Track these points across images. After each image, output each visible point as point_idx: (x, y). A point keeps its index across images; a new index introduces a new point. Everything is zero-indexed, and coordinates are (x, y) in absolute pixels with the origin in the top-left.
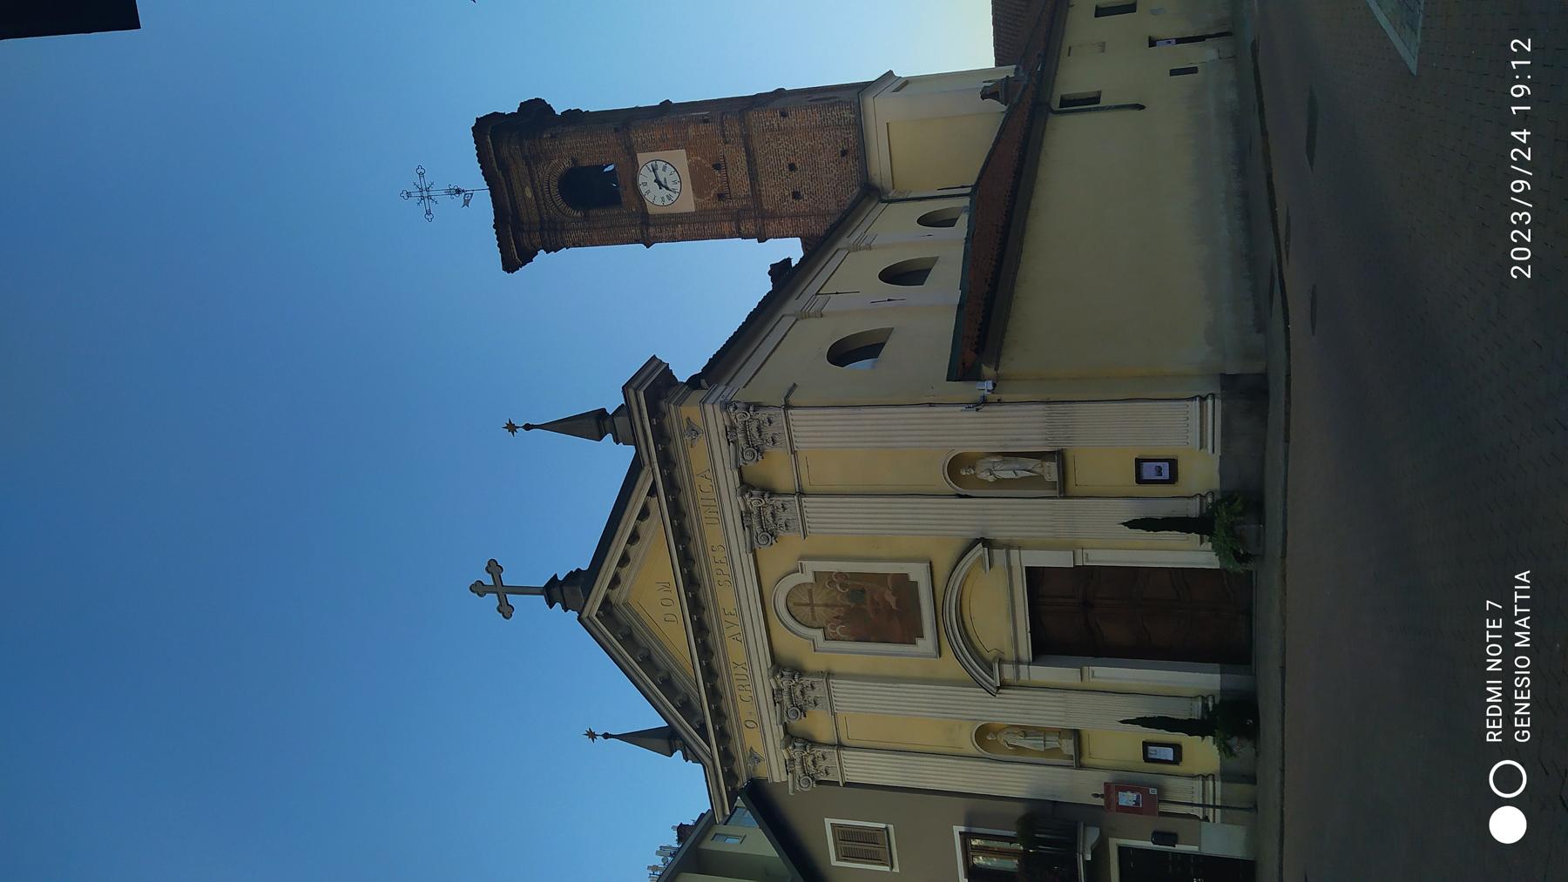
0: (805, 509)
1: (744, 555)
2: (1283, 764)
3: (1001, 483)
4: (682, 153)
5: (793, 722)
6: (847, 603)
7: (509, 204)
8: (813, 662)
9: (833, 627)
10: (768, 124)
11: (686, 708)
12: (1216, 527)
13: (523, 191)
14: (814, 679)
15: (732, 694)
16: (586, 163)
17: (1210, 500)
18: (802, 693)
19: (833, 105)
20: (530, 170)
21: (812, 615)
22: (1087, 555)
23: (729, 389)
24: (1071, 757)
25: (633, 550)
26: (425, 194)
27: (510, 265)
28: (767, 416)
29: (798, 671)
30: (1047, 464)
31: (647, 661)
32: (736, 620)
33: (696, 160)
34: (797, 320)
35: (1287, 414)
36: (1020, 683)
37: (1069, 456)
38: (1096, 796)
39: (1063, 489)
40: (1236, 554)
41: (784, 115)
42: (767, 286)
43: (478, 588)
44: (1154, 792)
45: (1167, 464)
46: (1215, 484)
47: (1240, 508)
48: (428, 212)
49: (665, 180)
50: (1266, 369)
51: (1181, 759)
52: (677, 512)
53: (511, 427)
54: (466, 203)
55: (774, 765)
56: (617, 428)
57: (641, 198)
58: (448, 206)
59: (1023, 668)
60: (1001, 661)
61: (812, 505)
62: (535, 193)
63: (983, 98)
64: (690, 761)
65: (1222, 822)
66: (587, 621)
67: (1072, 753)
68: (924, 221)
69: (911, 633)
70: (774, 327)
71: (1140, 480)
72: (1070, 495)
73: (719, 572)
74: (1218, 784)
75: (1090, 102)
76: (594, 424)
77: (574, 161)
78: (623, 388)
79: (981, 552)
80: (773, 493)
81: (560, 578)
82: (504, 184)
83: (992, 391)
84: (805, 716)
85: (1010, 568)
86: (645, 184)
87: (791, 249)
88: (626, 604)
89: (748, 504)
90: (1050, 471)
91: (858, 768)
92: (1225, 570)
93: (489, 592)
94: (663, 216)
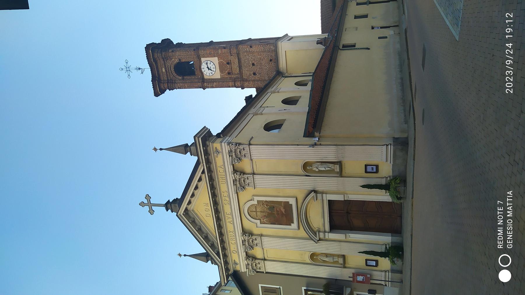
0: (255, 179)
1: (234, 195)
2: (411, 267)
3: (320, 172)
6: (268, 211)
7: (157, 75)
8: (256, 231)
10: (245, 50)
11: (213, 246)
12: (390, 188)
13: (162, 69)
14: (257, 237)
15: (228, 242)
16: (184, 61)
17: (389, 179)
18: (252, 241)
19: (267, 44)
22: (348, 196)
23: (230, 138)
24: (342, 264)
25: (196, 192)
26: (128, 69)
27: (157, 94)
29: (251, 234)
30: (336, 166)
31: (200, 230)
34: (254, 115)
35: (414, 151)
37: (343, 164)
38: (350, 277)
39: (341, 174)
40: (397, 197)
41: (251, 47)
42: (244, 104)
43: (142, 204)
44: (369, 276)
45: (375, 166)
46: (391, 174)
47: (399, 182)
48: (129, 75)
49: (210, 67)
50: (408, 136)
51: (378, 265)
52: (211, 179)
53: (155, 149)
54: (142, 73)
55: (242, 266)
56: (192, 152)
58: (136, 74)
59: (326, 234)
60: (319, 232)
62: (166, 71)
63: (317, 44)
64: (213, 264)
65: (391, 286)
66: (179, 216)
67: (342, 263)
68: (297, 84)
69: (289, 222)
70: (246, 117)
72: (343, 176)
73: (225, 200)
74: (390, 274)
75: (352, 46)
76: (184, 149)
77: (180, 60)
78: (194, 137)
79: (313, 195)
80: (244, 173)
81: (171, 201)
83: (318, 141)
84: (253, 249)
85: (323, 200)
86: (204, 68)
87: (253, 92)
88: (193, 210)
90: (337, 168)
91: (271, 267)
92: (394, 202)
94: (209, 79)
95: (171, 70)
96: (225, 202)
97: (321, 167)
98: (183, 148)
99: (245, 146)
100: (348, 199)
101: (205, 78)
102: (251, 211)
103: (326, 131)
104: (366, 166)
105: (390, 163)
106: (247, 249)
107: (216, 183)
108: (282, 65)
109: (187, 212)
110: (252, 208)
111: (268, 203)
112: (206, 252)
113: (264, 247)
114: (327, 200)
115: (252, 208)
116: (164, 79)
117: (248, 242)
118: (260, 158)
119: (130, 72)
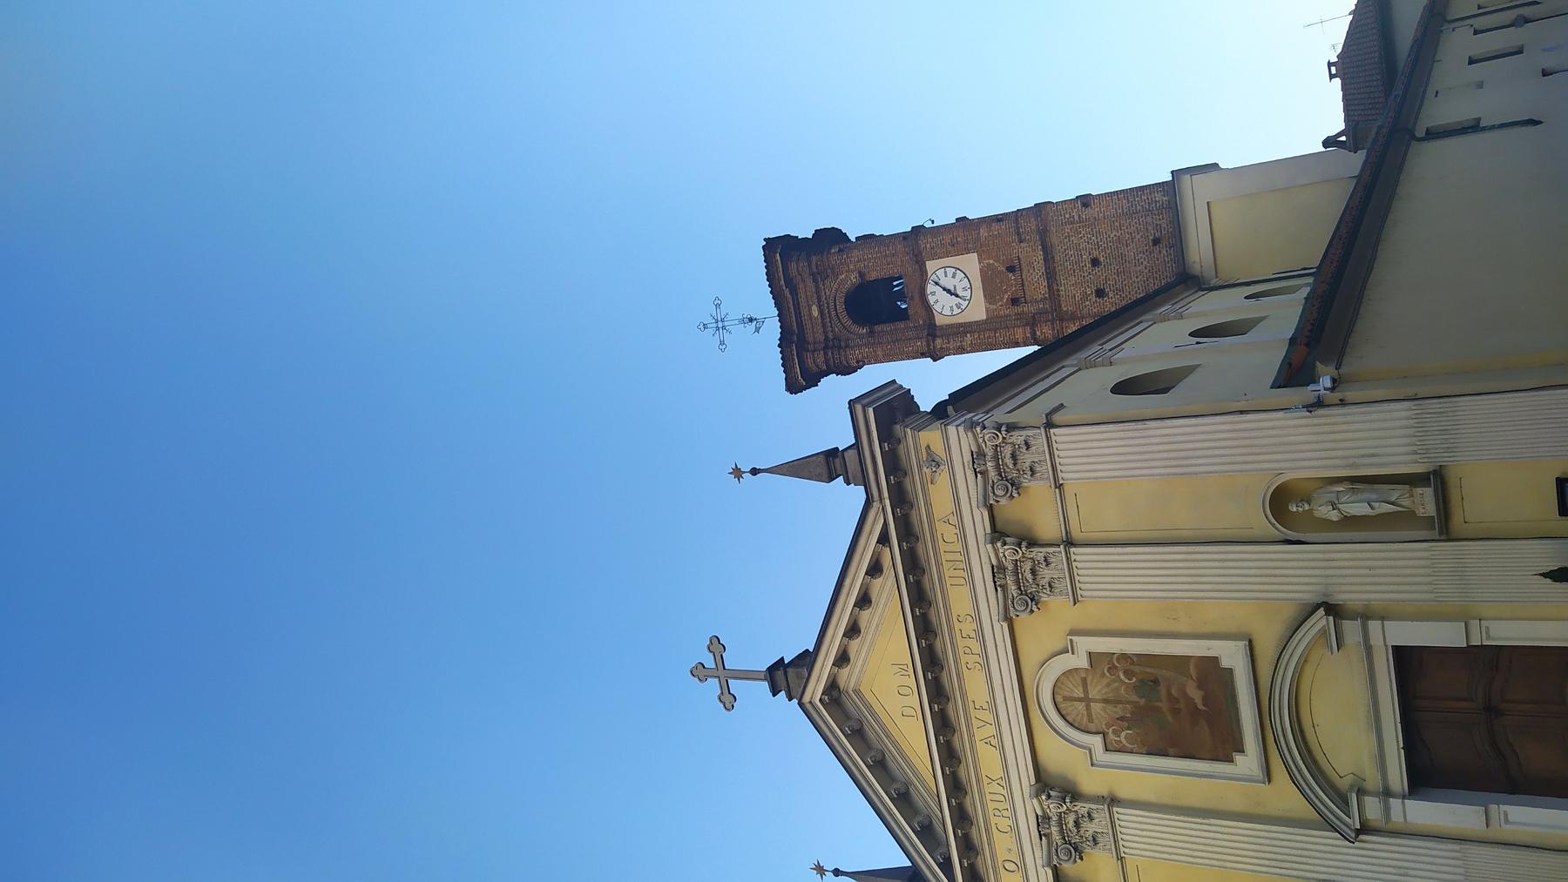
3: (1349, 522)
5: (1065, 865)
6: (1138, 700)
8: (1091, 781)
10: (1067, 216)
11: (927, 832)
13: (810, 310)
14: (1094, 806)
16: (873, 276)
18: (1077, 824)
20: (817, 287)
22: (1487, 628)
26: (720, 324)
27: (793, 387)
28: (1023, 438)
29: (1071, 793)
30: (1419, 490)
31: (880, 766)
32: (989, 718)
33: (989, 264)
36: (1390, 827)
37: (1452, 480)
39: (1443, 526)
43: (699, 672)
48: (722, 343)
49: (955, 287)
52: (914, 566)
53: (737, 473)
54: (757, 330)
57: (928, 309)
58: (740, 335)
59: (1395, 803)
60: (1361, 792)
61: (1084, 558)
62: (821, 312)
66: (809, 706)
69: (1225, 746)
73: (968, 651)
76: (828, 465)
77: (861, 275)
79: (1323, 622)
80: (1033, 543)
82: (791, 303)
83: (1333, 389)
84: (1081, 859)
85: (1368, 649)
86: (933, 293)
88: (857, 692)
89: (1001, 555)
93: (711, 677)
94: (951, 326)
95: (836, 310)
96: (971, 659)
97: (1352, 499)
98: (822, 459)
99: (1030, 432)
101: (937, 324)
102: (1066, 699)
103: (1365, 356)
106: (1057, 856)
107: (931, 582)
108: (1199, 250)
109: (835, 693)
110: (1071, 686)
111: (1133, 663)
112: (911, 865)
113: (1126, 850)
114: (1386, 646)
115: (1071, 686)
116: (815, 338)
117: (1060, 825)
118: (1088, 475)
119: (725, 331)
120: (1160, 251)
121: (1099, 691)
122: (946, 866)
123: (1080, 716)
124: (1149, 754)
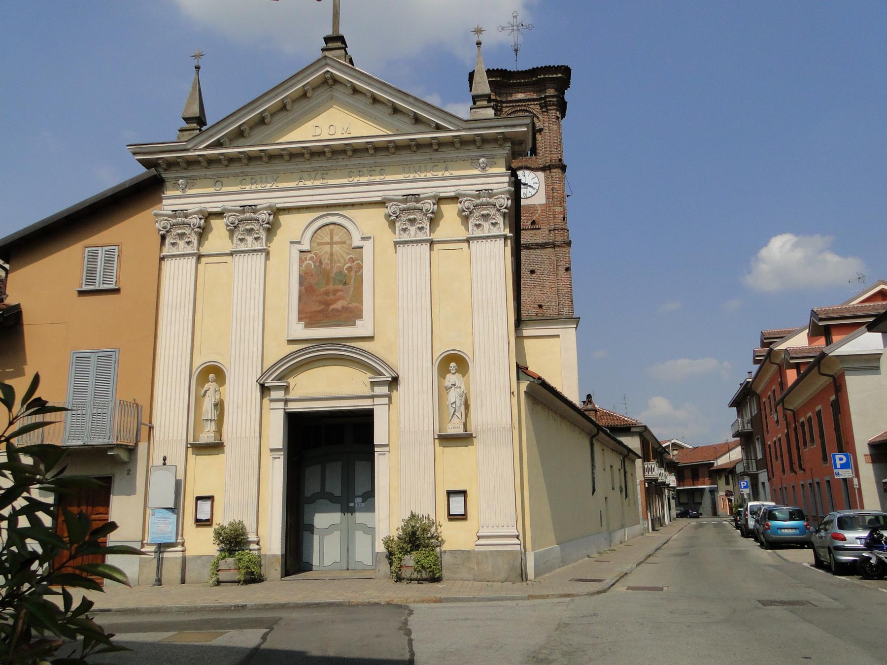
1: (381, 193)
4: (543, 201)
9: (312, 258)
21: (322, 243)
69: (309, 317)
71: (450, 493)
79: (387, 375)
100: (376, 453)
102: (332, 231)
104: (464, 493)
105: (476, 545)
110: (340, 234)
114: (374, 405)
115: (340, 234)
120: (535, 308)
121: (338, 251)
122: (218, 144)
123: (321, 238)
124: (301, 277)
